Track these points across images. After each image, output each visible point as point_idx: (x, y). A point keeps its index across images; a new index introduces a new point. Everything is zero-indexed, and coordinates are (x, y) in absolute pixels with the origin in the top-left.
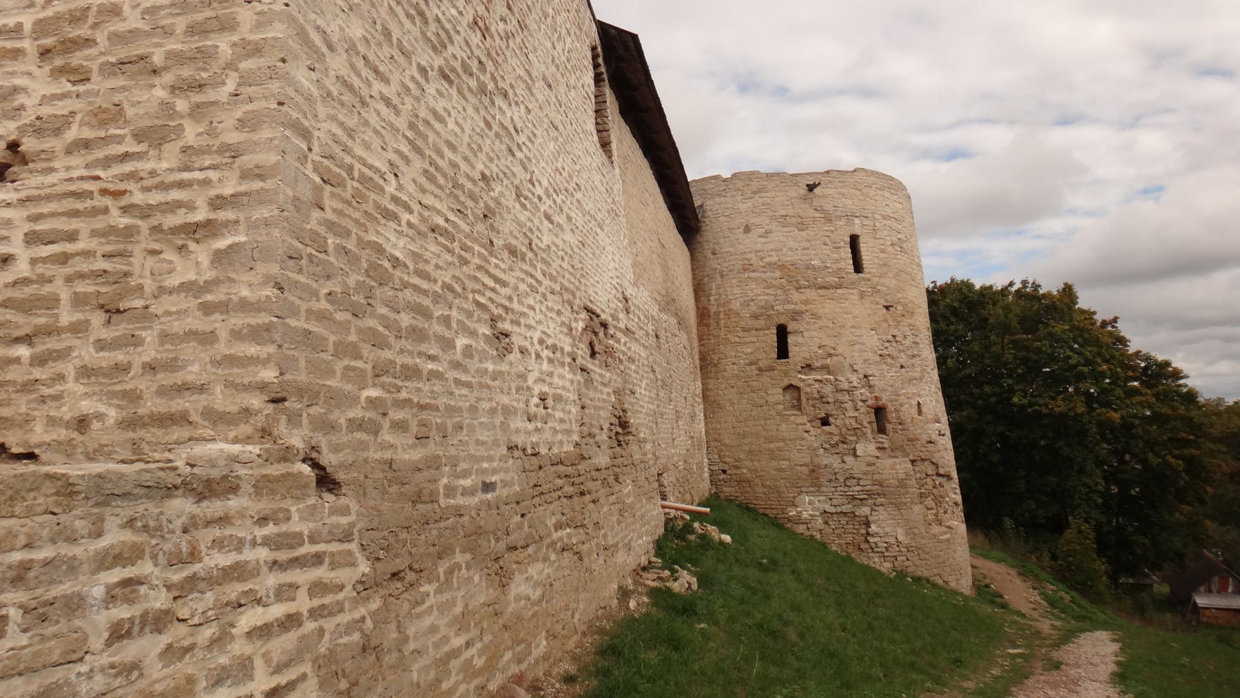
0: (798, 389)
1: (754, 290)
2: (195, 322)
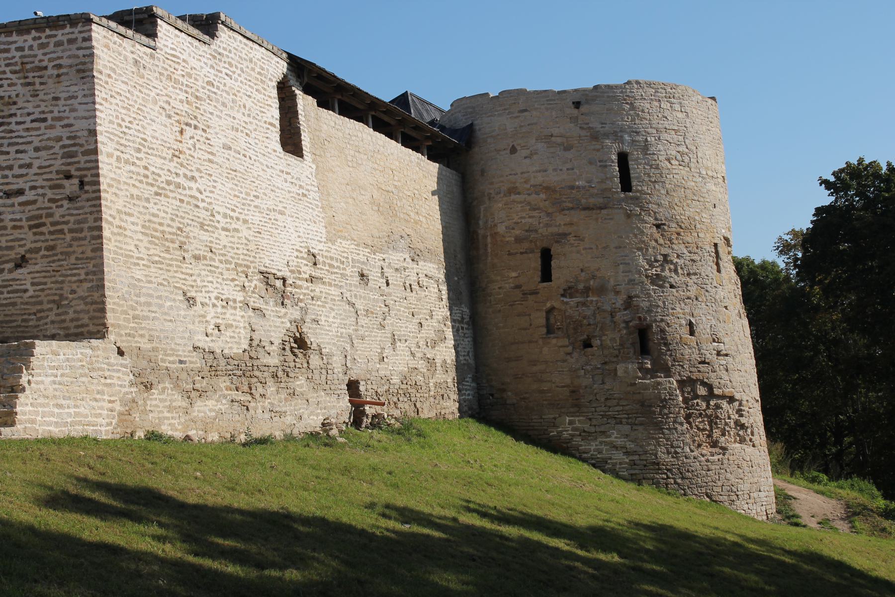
2: (82, 307)
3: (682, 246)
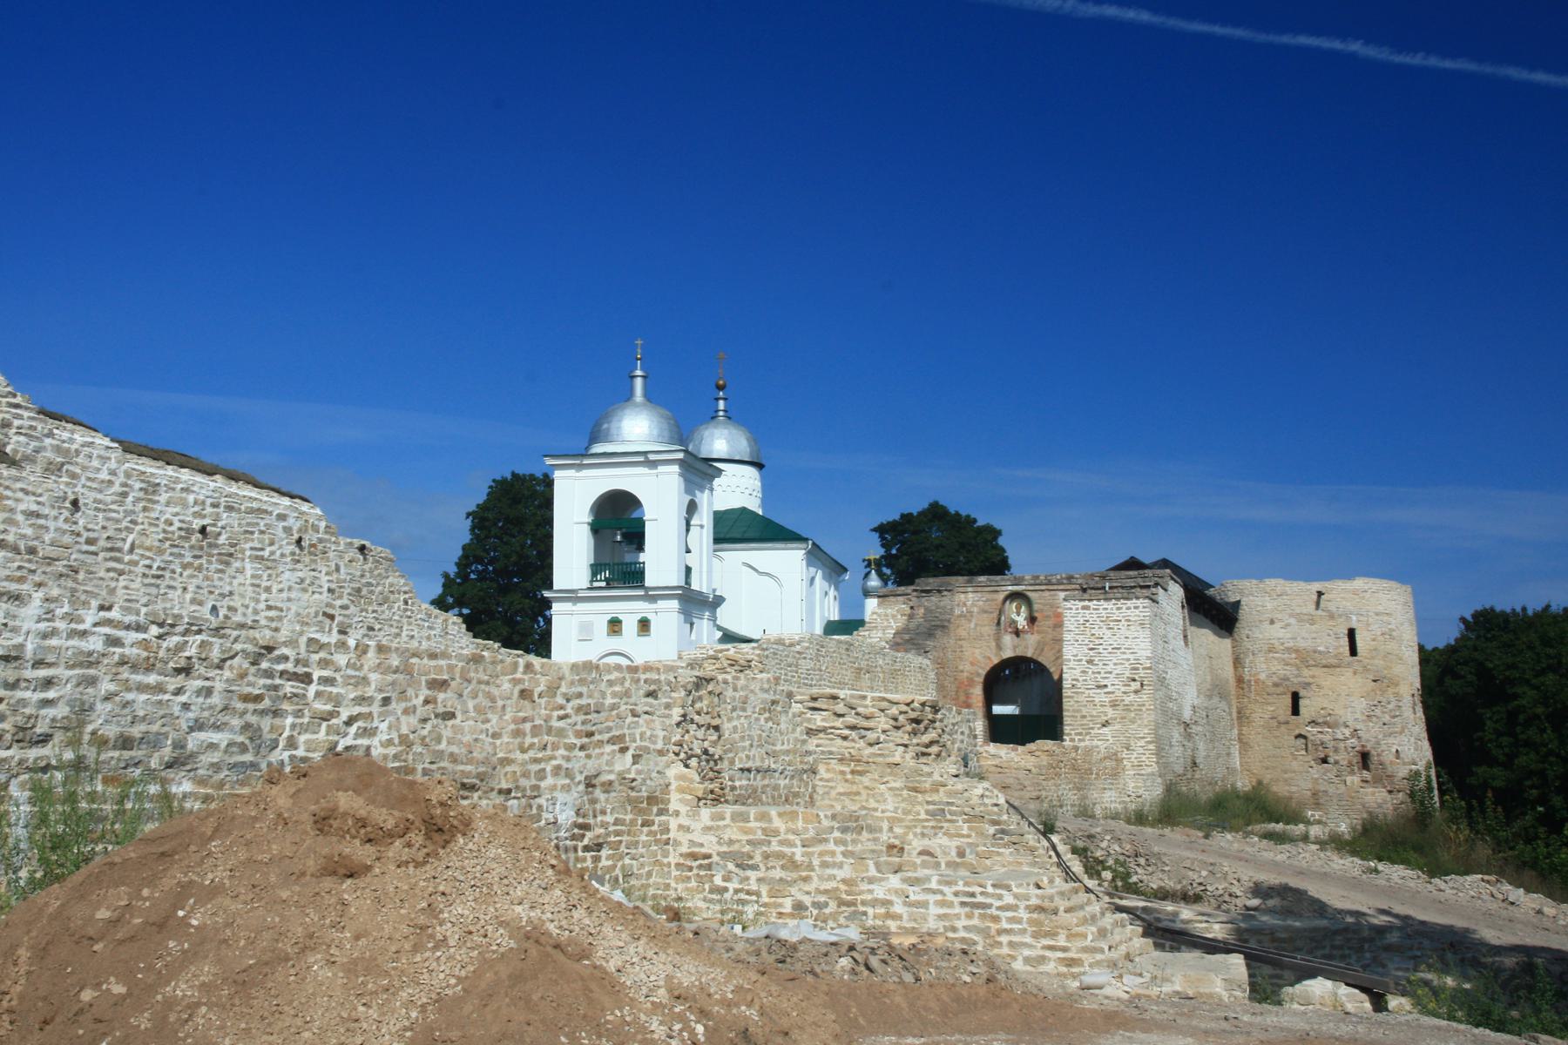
0: (1305, 737)
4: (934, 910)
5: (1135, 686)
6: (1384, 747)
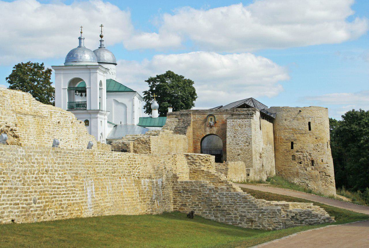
1: (287, 134)
3: (321, 143)
4: (225, 199)
5: (247, 144)
6: (318, 159)
